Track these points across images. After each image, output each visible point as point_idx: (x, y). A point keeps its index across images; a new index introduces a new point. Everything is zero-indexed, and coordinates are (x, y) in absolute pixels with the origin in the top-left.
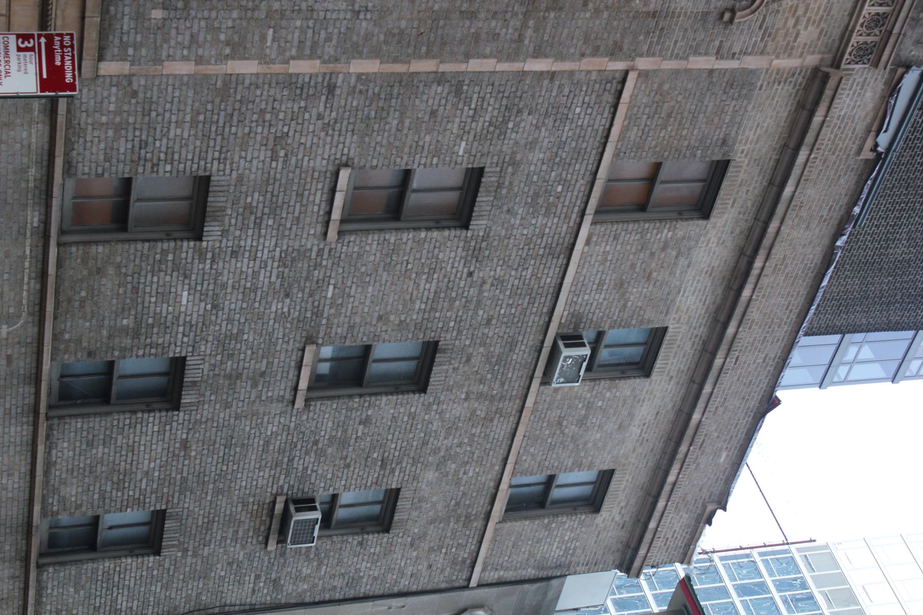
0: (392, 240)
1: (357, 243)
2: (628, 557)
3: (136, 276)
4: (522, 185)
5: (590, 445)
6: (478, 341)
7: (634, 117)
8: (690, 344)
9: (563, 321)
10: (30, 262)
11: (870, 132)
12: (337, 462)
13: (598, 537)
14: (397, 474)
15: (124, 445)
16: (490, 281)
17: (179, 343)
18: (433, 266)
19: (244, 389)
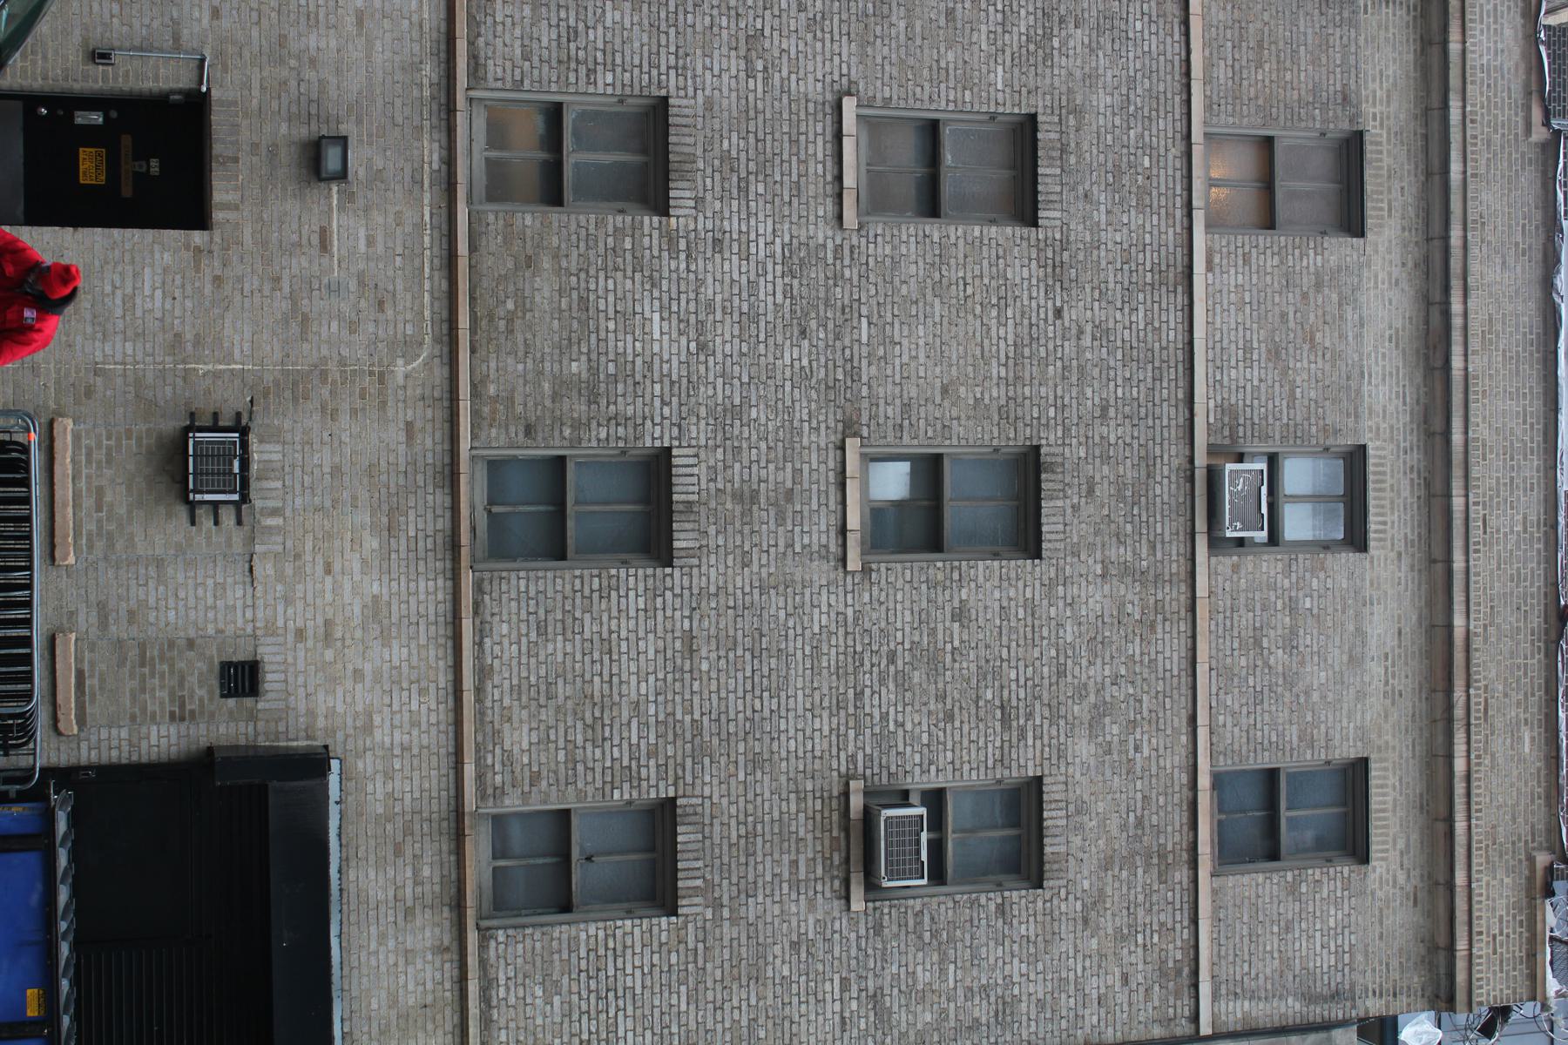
0: (936, 239)
1: (888, 239)
2: (1442, 971)
3: (583, 275)
4: (1095, 151)
5: (1315, 696)
6: (1097, 453)
7: (1215, 45)
8: (1407, 482)
9: (1212, 420)
10: (431, 236)
11: (1530, 93)
12: (932, 707)
13: (1381, 923)
14: (1030, 742)
15: (596, 637)
16: (1089, 328)
17: (657, 420)
18: (1003, 293)
19: (764, 516)
